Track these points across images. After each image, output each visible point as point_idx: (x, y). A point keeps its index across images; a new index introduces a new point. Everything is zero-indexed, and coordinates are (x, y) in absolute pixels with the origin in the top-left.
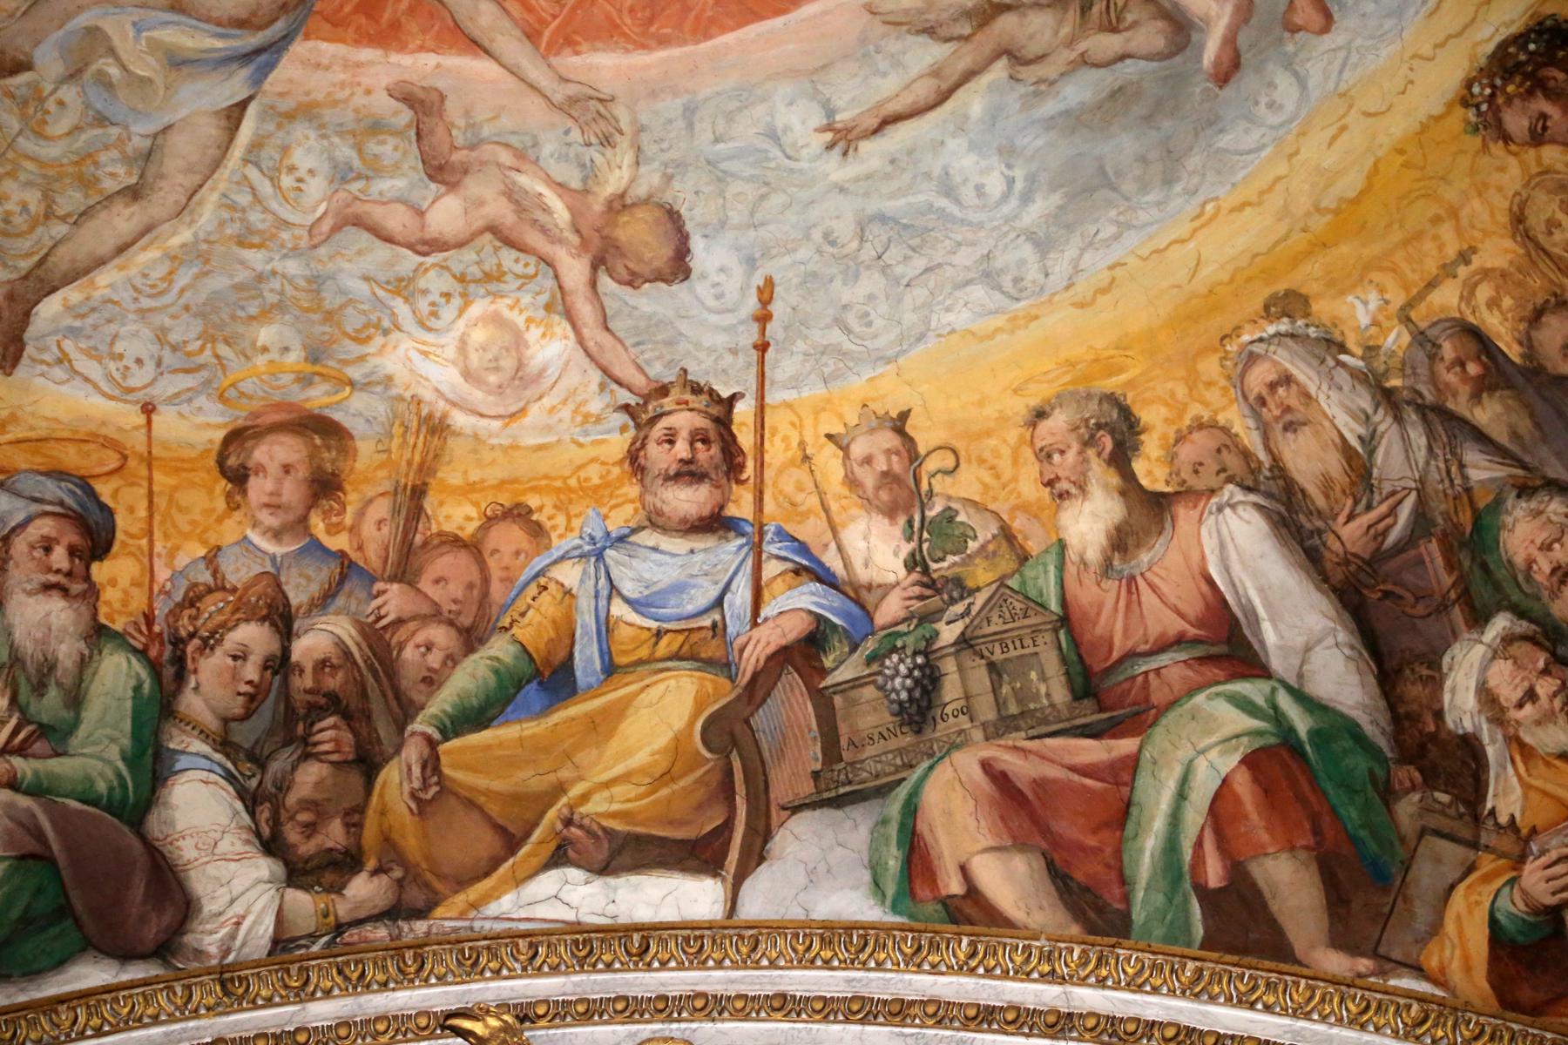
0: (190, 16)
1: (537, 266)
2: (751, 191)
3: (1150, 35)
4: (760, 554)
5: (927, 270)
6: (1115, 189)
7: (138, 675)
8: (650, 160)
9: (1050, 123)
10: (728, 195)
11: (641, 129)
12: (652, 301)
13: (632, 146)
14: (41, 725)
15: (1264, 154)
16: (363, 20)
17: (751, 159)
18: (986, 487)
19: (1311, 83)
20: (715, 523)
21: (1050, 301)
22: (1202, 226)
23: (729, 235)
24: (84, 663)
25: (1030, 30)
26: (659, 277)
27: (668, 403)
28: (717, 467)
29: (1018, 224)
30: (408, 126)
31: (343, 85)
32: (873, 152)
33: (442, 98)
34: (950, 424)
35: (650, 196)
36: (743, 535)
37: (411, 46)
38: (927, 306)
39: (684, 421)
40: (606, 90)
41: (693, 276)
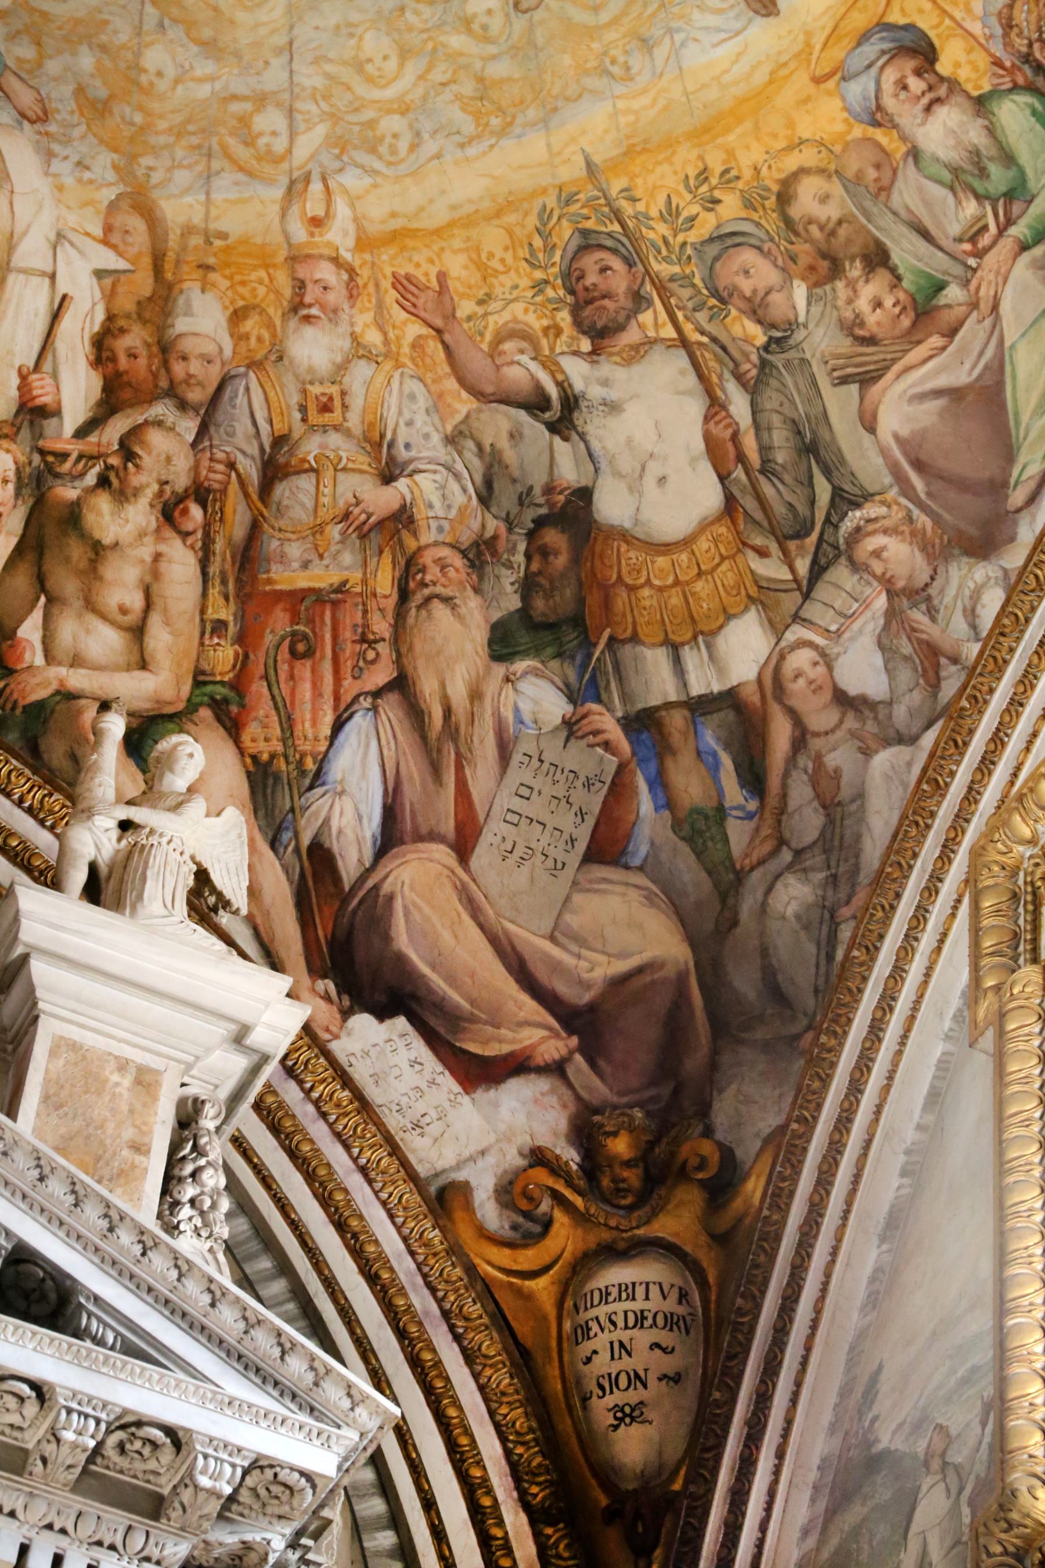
7: (1026, 104)
14: (1005, 195)
24: (991, 131)
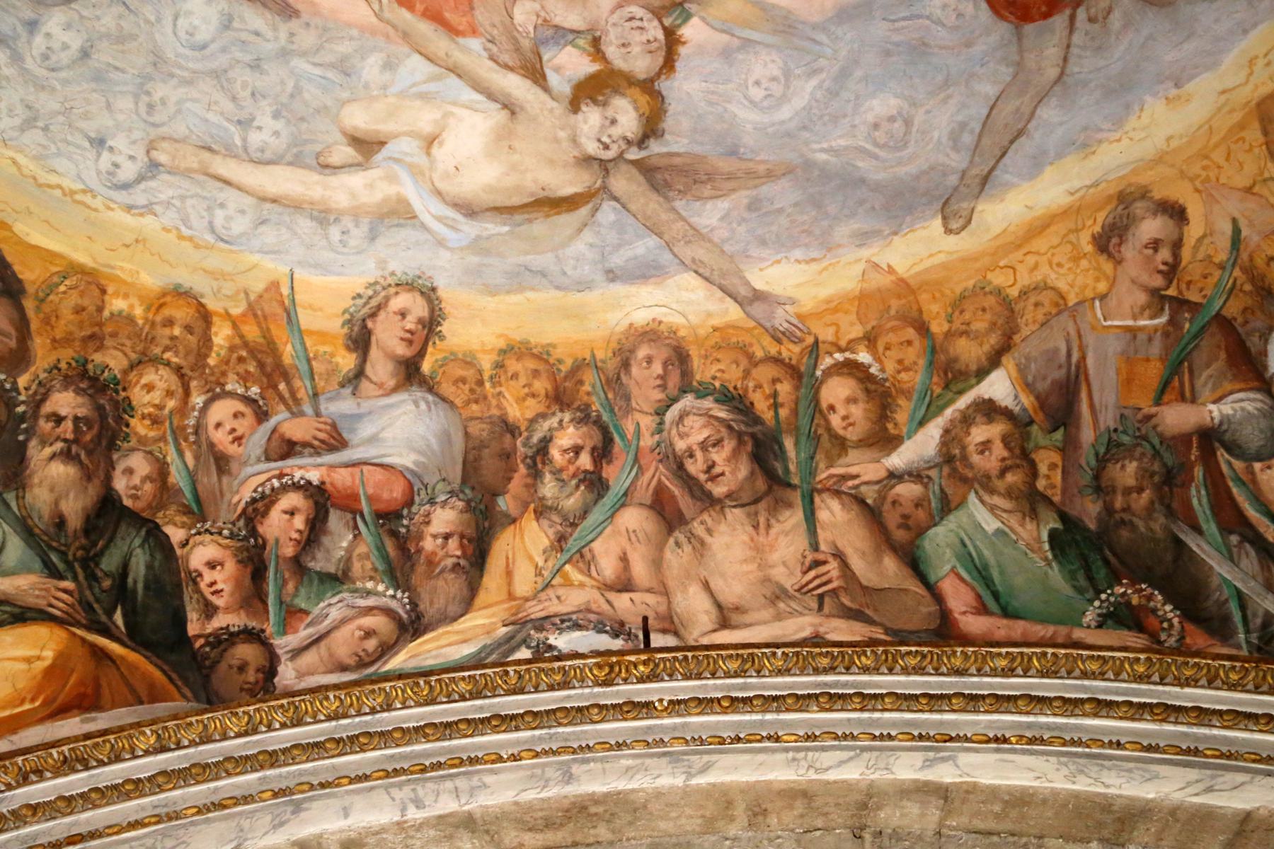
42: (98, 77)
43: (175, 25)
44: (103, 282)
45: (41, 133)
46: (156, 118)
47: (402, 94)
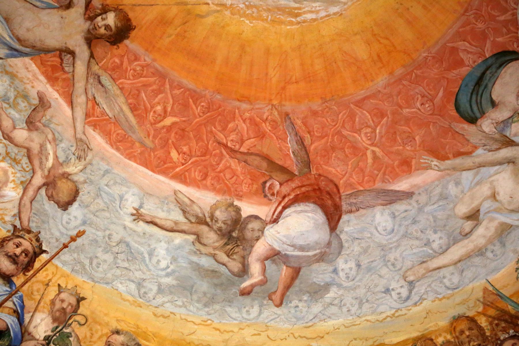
0: (8, 25)
1: (30, 170)
2: (102, 205)
3: (235, 266)
4: (10, 297)
5: (126, 268)
6: (191, 294)
8: (85, 173)
9: (191, 263)
10: (96, 201)
11: (91, 164)
12: (50, 207)
13: (84, 165)
15: (235, 322)
16: (50, 69)
17: (110, 198)
18: (86, 337)
19: (262, 316)
20: (8, 279)
21: (148, 306)
22: (203, 325)
23: (86, 211)
25: (208, 236)
26: (58, 203)
27: (27, 236)
28: (22, 264)
29: (159, 279)
30: (34, 105)
31: (28, 79)
32: (142, 226)
33: (50, 107)
34: (93, 313)
35: (76, 182)
36: (11, 288)
37: (55, 88)
38: (117, 277)
39: (26, 245)
40: (92, 146)
41: (67, 211)
42: (369, 269)
43: (378, 231)
44: (429, 337)
45: (367, 304)
46: (398, 267)
47: (471, 189)
